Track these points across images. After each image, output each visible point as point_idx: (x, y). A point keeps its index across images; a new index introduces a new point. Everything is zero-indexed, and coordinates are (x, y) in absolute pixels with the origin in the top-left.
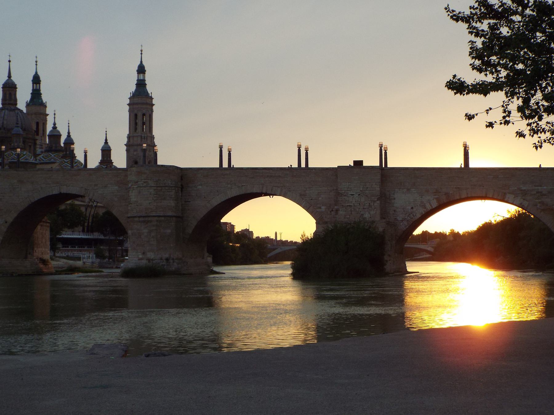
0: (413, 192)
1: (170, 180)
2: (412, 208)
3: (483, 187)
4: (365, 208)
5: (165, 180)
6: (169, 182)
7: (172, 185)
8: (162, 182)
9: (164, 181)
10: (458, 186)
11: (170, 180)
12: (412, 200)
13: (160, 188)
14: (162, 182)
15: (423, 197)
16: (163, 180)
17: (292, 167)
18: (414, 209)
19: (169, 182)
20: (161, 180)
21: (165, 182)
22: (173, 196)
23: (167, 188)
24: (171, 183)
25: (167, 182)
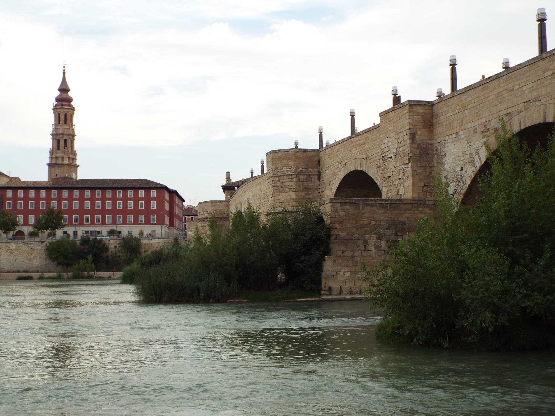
0: (462, 136)
1: (290, 167)
2: (462, 169)
3: (540, 100)
4: (400, 177)
5: (284, 168)
6: (288, 170)
7: (292, 173)
8: (280, 171)
9: (282, 169)
10: (509, 111)
11: (290, 167)
12: (461, 154)
13: (277, 179)
14: (280, 171)
15: (472, 144)
16: (281, 168)
17: (375, 125)
18: (464, 171)
19: (288, 170)
20: (279, 168)
21: (283, 170)
22: (294, 187)
23: (285, 177)
24: (291, 170)
25: (286, 170)
